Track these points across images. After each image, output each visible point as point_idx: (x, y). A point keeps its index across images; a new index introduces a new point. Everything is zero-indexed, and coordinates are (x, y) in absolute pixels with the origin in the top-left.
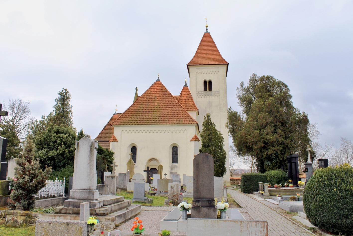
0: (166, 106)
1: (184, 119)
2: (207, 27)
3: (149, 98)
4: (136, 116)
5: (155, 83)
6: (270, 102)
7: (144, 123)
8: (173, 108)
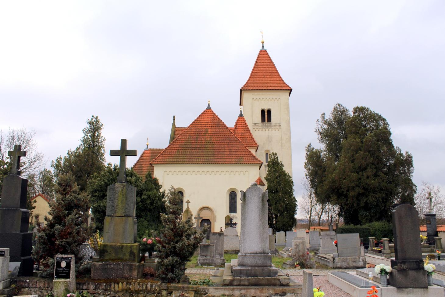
0: (221, 141)
1: (244, 158)
2: (263, 42)
3: (198, 130)
4: (183, 153)
5: (204, 111)
6: (370, 138)
7: (193, 162)
8: (230, 144)
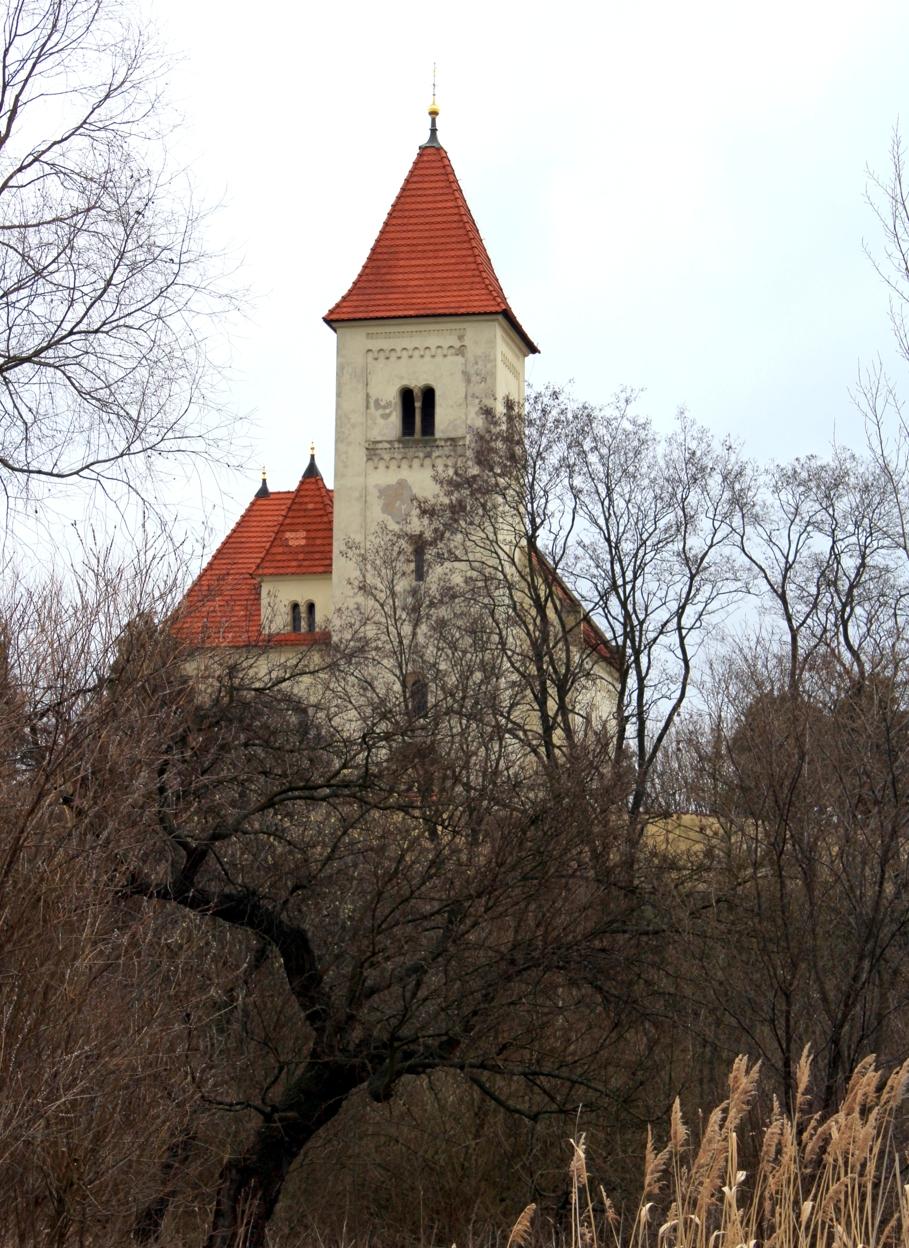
2: (434, 114)
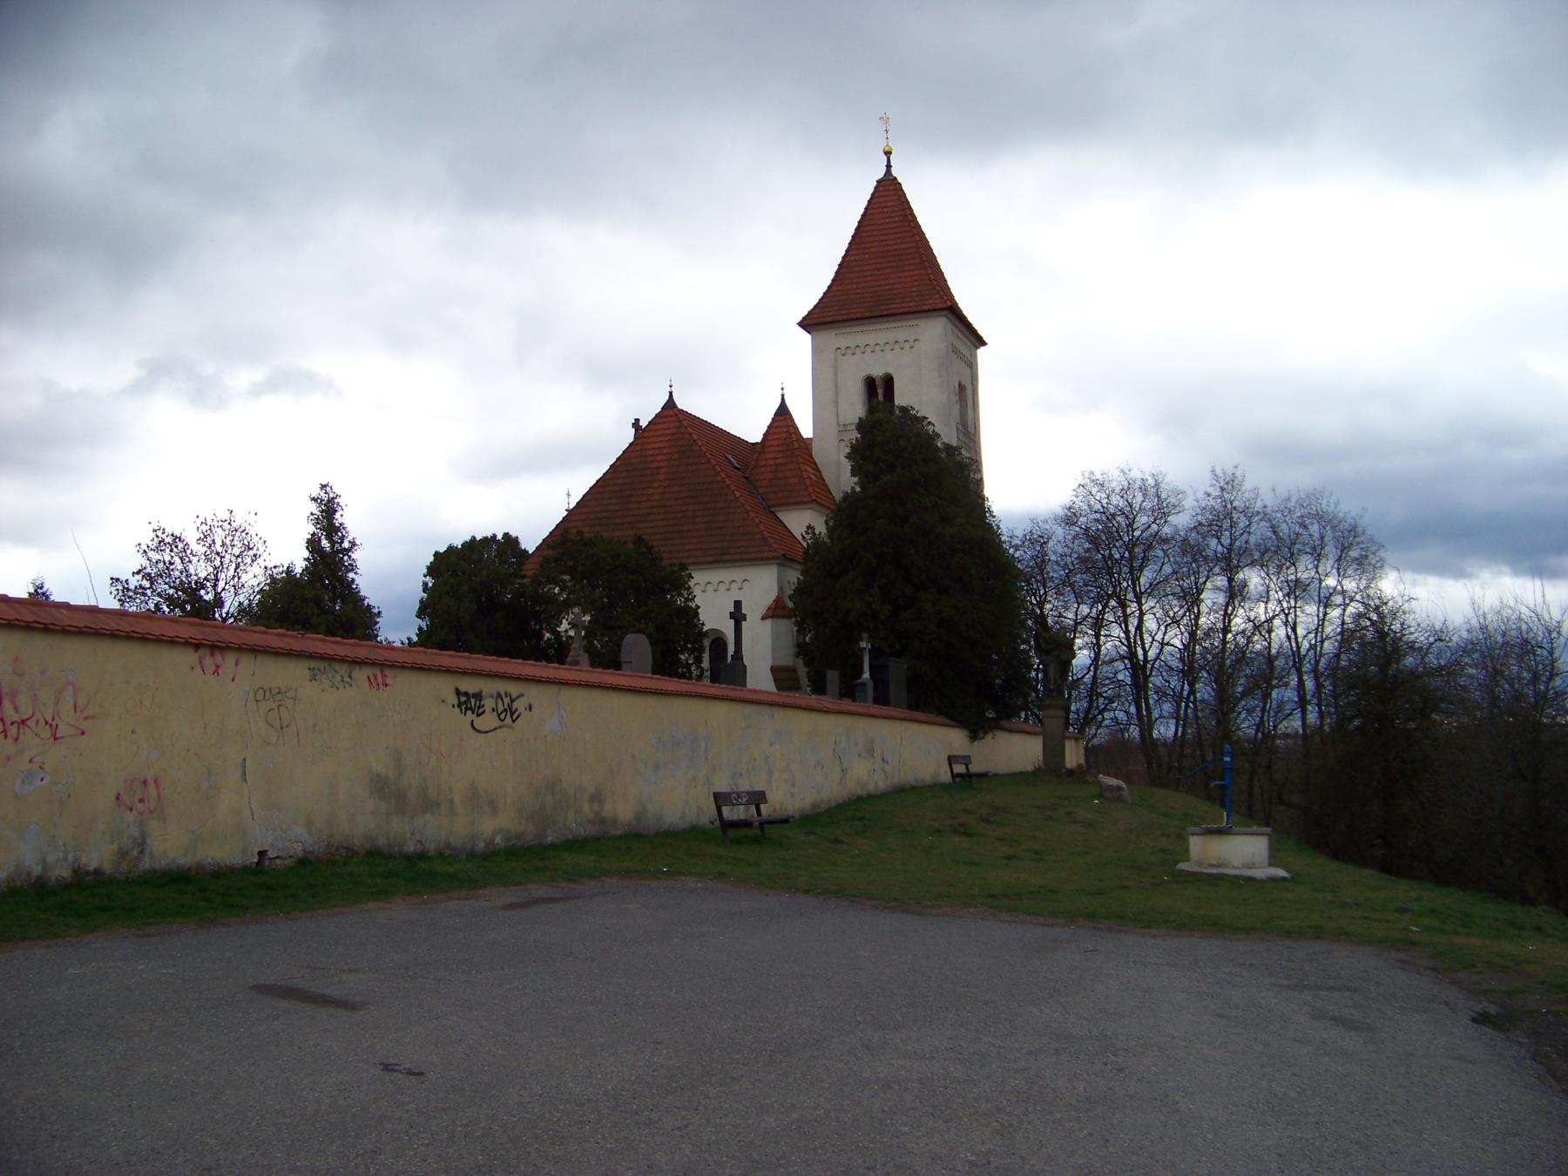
2: (888, 153)
